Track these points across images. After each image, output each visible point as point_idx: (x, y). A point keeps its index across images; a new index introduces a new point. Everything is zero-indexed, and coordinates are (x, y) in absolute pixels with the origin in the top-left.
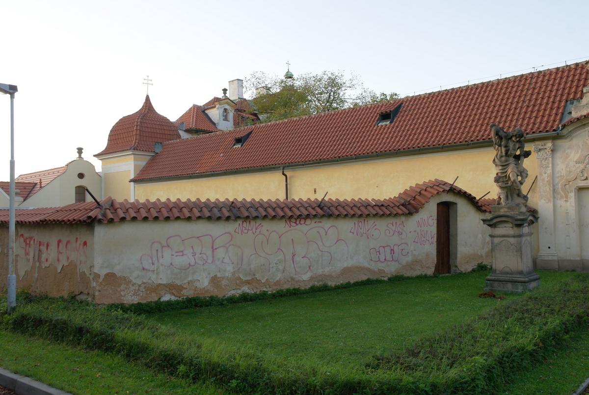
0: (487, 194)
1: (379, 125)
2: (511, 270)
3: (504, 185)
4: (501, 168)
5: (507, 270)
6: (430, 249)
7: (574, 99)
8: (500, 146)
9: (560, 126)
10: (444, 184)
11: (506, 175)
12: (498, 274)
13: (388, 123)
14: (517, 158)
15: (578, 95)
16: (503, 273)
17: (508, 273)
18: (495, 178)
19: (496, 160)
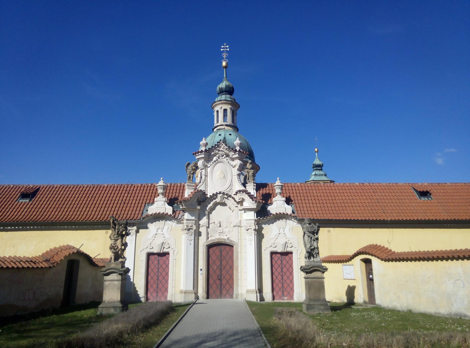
0: (98, 255)
1: (20, 201)
2: (113, 300)
3: (114, 251)
4: (114, 241)
5: (112, 301)
6: (61, 291)
7: (149, 203)
8: (115, 229)
9: (142, 218)
10: (73, 248)
11: (116, 246)
12: (107, 303)
13: (28, 201)
14: (123, 236)
15: (151, 201)
16: (108, 303)
17: (112, 302)
18: (110, 246)
19: (112, 237)
